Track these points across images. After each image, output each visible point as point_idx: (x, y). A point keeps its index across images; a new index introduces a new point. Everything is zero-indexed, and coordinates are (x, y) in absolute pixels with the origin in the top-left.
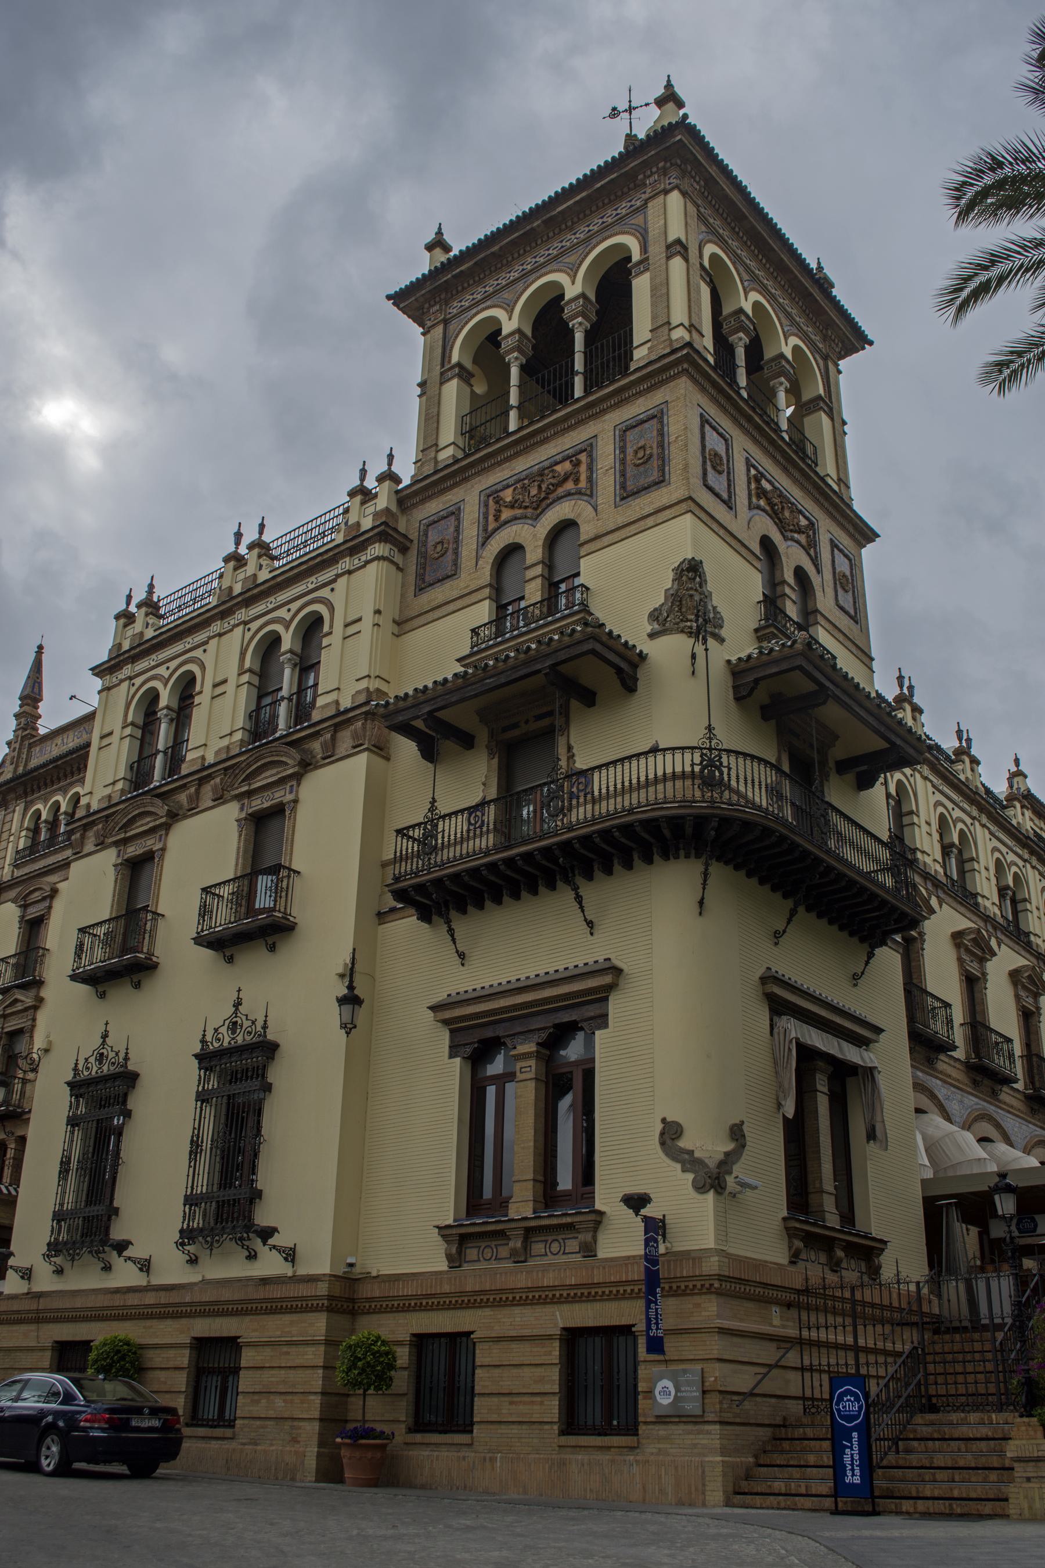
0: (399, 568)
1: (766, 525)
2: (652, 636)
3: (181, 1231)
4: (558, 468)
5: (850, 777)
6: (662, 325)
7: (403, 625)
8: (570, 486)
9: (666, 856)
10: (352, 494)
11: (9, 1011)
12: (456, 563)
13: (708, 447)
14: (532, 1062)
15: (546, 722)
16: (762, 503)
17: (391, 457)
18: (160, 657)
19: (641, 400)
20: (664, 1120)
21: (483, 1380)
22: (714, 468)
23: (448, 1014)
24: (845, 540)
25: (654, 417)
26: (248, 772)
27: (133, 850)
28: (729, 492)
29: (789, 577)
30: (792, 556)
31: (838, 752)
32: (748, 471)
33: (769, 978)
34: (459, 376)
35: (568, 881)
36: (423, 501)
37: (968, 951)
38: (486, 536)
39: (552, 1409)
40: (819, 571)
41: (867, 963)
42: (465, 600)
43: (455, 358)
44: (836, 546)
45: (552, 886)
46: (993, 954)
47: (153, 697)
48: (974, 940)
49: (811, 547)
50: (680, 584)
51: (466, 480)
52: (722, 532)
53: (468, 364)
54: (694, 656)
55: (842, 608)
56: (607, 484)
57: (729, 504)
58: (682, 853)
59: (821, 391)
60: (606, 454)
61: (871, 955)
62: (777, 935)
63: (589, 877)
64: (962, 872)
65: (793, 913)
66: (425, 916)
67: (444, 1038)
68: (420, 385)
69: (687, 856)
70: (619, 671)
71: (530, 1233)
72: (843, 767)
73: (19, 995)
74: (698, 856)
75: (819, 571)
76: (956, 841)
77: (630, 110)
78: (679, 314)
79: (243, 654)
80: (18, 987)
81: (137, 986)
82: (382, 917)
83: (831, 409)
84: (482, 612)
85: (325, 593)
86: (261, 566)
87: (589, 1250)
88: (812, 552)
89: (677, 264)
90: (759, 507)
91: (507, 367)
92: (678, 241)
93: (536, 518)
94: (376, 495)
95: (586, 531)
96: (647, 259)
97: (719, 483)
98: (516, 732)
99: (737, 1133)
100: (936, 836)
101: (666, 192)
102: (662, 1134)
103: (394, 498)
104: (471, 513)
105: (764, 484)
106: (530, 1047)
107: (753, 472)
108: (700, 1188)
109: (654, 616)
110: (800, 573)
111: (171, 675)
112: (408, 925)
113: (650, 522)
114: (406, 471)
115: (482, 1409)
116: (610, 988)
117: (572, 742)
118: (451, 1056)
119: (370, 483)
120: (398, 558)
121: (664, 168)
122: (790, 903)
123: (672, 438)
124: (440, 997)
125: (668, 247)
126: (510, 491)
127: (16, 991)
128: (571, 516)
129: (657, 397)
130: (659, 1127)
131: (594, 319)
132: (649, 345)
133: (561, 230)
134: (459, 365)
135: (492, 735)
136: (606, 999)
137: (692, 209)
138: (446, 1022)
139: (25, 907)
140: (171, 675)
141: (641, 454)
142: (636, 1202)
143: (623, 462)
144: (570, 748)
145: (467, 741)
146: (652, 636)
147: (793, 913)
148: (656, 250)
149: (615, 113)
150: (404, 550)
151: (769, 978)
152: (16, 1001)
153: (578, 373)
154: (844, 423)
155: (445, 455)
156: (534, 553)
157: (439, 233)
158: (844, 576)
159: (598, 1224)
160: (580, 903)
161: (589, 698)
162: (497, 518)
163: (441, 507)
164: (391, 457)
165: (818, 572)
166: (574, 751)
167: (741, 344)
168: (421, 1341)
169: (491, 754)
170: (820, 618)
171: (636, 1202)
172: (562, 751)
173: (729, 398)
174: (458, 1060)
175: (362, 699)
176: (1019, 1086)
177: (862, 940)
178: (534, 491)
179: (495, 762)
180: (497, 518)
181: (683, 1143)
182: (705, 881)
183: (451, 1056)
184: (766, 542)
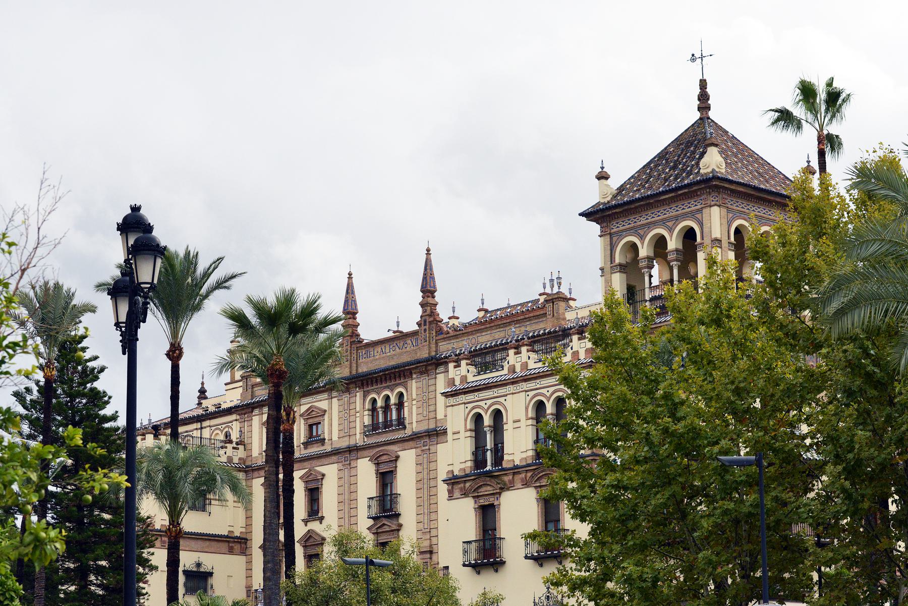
11: (380, 530)
18: (480, 395)
26: (539, 476)
27: (483, 502)
47: (478, 418)
73: (385, 521)
77: (702, 57)
79: (527, 408)
80: (385, 517)
81: (496, 571)
86: (529, 358)
96: (703, 243)
101: (711, 206)
111: (488, 408)
121: (709, 192)
125: (712, 241)
127: (383, 519)
134: (620, 265)
137: (724, 211)
139: (377, 464)
140: (488, 408)
148: (707, 241)
149: (693, 58)
152: (384, 525)
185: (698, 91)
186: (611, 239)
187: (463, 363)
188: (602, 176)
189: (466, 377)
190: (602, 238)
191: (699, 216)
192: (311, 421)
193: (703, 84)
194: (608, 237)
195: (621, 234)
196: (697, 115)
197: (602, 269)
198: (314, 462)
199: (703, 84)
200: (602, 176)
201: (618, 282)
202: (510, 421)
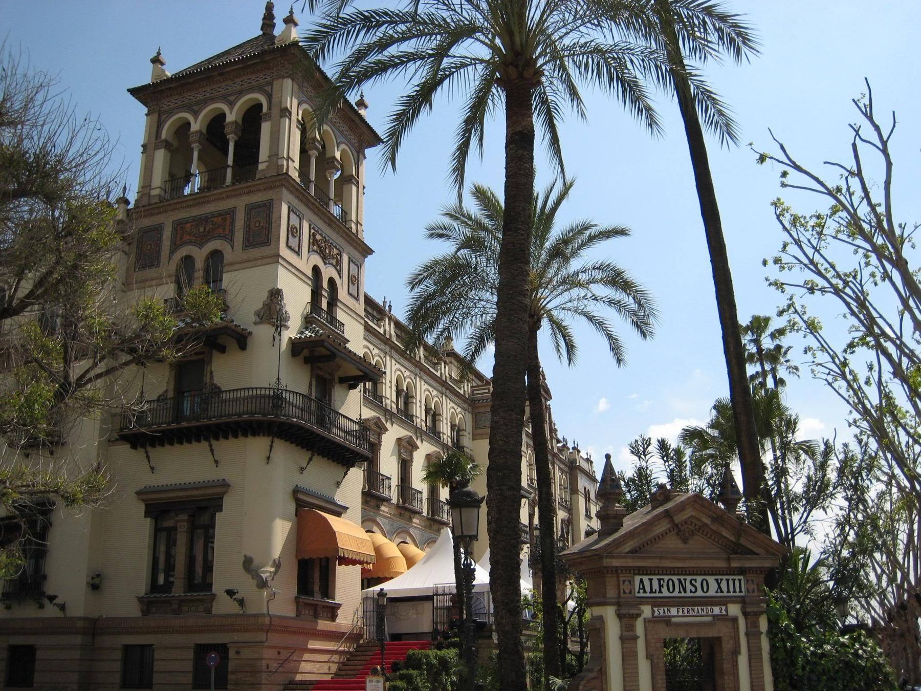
0: (126, 254)
1: (316, 260)
2: (255, 323)
3: (3, 594)
4: (215, 219)
5: (346, 385)
7: (127, 285)
8: (221, 231)
12: (158, 257)
13: (291, 223)
14: (186, 524)
15: (200, 357)
16: (315, 248)
19: (260, 194)
20: (245, 556)
21: (157, 666)
22: (293, 235)
23: (145, 497)
24: (357, 255)
25: (265, 206)
28: (299, 247)
29: (325, 285)
30: (328, 272)
31: (340, 373)
32: (310, 231)
34: (165, 148)
35: (207, 439)
37: (404, 447)
38: (175, 247)
39: (189, 678)
41: (344, 477)
43: (164, 136)
44: (352, 261)
45: (199, 441)
46: (417, 448)
48: (408, 442)
49: (338, 265)
50: (271, 300)
51: (165, 211)
52: (293, 270)
53: (170, 140)
54: (274, 338)
55: (351, 295)
56: (239, 236)
57: (298, 253)
58: (261, 434)
59: (354, 174)
60: (240, 223)
61: (346, 474)
62: (302, 469)
63: (217, 439)
64: (406, 404)
65: (310, 460)
66: (134, 447)
67: (142, 507)
68: (142, 146)
69: (264, 435)
71: (182, 602)
72: (342, 380)
74: (268, 436)
76: (405, 389)
82: (110, 442)
83: (358, 183)
87: (208, 611)
88: (338, 268)
90: (314, 251)
91: (192, 150)
95: (228, 256)
97: (294, 243)
100: (394, 388)
101: (283, 77)
102: (244, 562)
103: (125, 214)
104: (167, 234)
105: (318, 237)
106: (185, 517)
107: (312, 231)
109: (257, 314)
110: (331, 281)
112: (124, 449)
113: (259, 262)
114: (132, 197)
115: (156, 678)
116: (224, 493)
117: (213, 369)
118: (146, 516)
120: (127, 249)
122: (309, 454)
123: (274, 220)
124: (141, 486)
126: (189, 225)
128: (220, 248)
129: (269, 195)
130: (243, 559)
131: (239, 133)
132: (267, 164)
133: (227, 80)
134: (166, 141)
136: (222, 498)
138: (144, 500)
141: (257, 225)
142: (230, 593)
143: (249, 226)
144: (211, 372)
147: (310, 460)
148: (275, 112)
153: (229, 166)
154: (364, 187)
155: (154, 192)
156: (199, 264)
157: (159, 54)
158: (354, 276)
159: (213, 600)
160: (212, 452)
161: (223, 350)
162: (181, 238)
165: (340, 277)
166: (214, 374)
167: (314, 156)
168: (127, 648)
170: (339, 304)
171: (230, 593)
173: (304, 195)
174: (149, 519)
176: (425, 514)
177: (343, 465)
178: (202, 229)
179: (174, 371)
180: (181, 238)
182: (271, 448)
183: (146, 516)
184: (316, 270)
186: (159, 116)
188: (156, 60)
190: (149, 117)
191: (268, 89)
194: (155, 116)
195: (170, 113)
197: (144, 146)
200: (156, 60)
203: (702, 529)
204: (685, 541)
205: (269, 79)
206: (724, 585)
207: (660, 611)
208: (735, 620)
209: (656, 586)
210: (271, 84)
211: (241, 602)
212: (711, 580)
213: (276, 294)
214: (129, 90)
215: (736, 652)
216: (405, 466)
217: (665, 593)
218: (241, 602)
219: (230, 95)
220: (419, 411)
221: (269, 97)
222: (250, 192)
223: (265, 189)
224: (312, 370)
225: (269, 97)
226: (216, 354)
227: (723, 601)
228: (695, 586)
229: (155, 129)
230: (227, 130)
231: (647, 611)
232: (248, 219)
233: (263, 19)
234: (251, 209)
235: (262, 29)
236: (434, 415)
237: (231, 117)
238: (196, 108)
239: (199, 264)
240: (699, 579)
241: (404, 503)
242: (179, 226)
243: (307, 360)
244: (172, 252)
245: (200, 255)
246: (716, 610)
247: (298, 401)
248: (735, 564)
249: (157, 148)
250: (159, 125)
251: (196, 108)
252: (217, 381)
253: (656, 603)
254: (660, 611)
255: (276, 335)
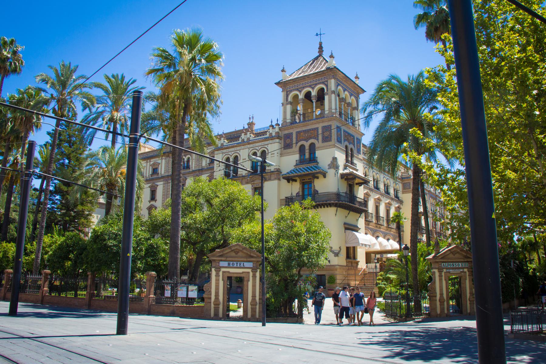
1: (346, 143)
2: (328, 169)
5: (358, 186)
6: (330, 108)
9: (330, 207)
10: (270, 126)
17: (277, 120)
19: (326, 123)
30: (350, 146)
33: (345, 224)
36: (284, 130)
40: (354, 147)
42: (293, 153)
51: (292, 128)
56: (320, 137)
59: (356, 106)
62: (346, 217)
70: (323, 175)
72: (357, 184)
75: (354, 147)
77: (320, 34)
78: (333, 107)
84: (297, 157)
85: (266, 146)
89: (333, 96)
92: (333, 91)
93: (307, 141)
94: (275, 128)
95: (317, 145)
98: (304, 181)
99: (340, 248)
101: (331, 79)
108: (335, 256)
109: (329, 165)
110: (351, 150)
113: (328, 147)
114: (280, 122)
119: (274, 124)
122: (348, 211)
134: (290, 102)
135: (300, 180)
144: (314, 186)
145: (296, 181)
146: (328, 169)
148: (329, 91)
149: (317, 35)
150: (281, 140)
151: (345, 224)
156: (307, 147)
161: (318, 178)
163: (288, 133)
164: (277, 120)
169: (300, 184)
172: (313, 185)
175: (276, 170)
176: (385, 225)
178: (307, 135)
181: (333, 249)
184: (346, 147)
185: (318, 46)
186: (287, 92)
187: (222, 139)
188: (283, 71)
189: (223, 144)
191: (326, 83)
192: (154, 167)
193: (321, 44)
194: (286, 93)
195: (291, 91)
196: (318, 54)
197: (283, 104)
198: (154, 181)
199: (321, 44)
201: (289, 108)
202: (241, 159)
203: (458, 252)
204: (454, 255)
205: (326, 80)
206: (463, 265)
207: (448, 270)
208: (465, 272)
209: (447, 265)
210: (327, 81)
211: (329, 261)
212: (460, 264)
213: (335, 159)
214: (275, 83)
215: (466, 279)
216: (377, 208)
217: (449, 266)
218: (329, 261)
219: (312, 85)
220: (382, 186)
221: (327, 86)
222: (323, 122)
223: (328, 121)
224: (347, 182)
225: (327, 86)
226: (316, 180)
227: (463, 268)
228: (456, 265)
229: (286, 97)
230: (312, 99)
231: (445, 270)
232: (323, 133)
233: (319, 49)
234: (324, 128)
235: (319, 52)
236: (387, 187)
237: (314, 93)
238: (300, 90)
239: (307, 147)
240: (457, 263)
241: (377, 222)
242: (298, 133)
243: (346, 180)
244: (297, 143)
245: (307, 144)
246: (461, 270)
247: (344, 195)
248: (466, 260)
249: (287, 104)
250: (287, 96)
251: (300, 90)
252: (317, 188)
253: (447, 269)
254: (448, 270)
255: (336, 173)
